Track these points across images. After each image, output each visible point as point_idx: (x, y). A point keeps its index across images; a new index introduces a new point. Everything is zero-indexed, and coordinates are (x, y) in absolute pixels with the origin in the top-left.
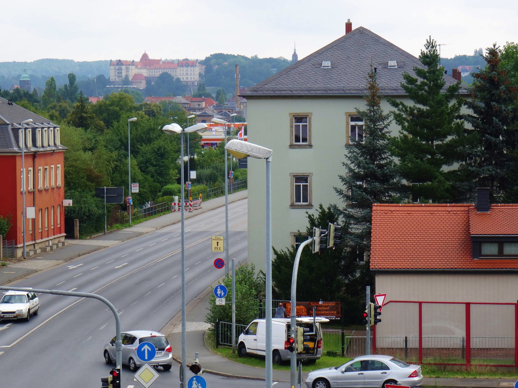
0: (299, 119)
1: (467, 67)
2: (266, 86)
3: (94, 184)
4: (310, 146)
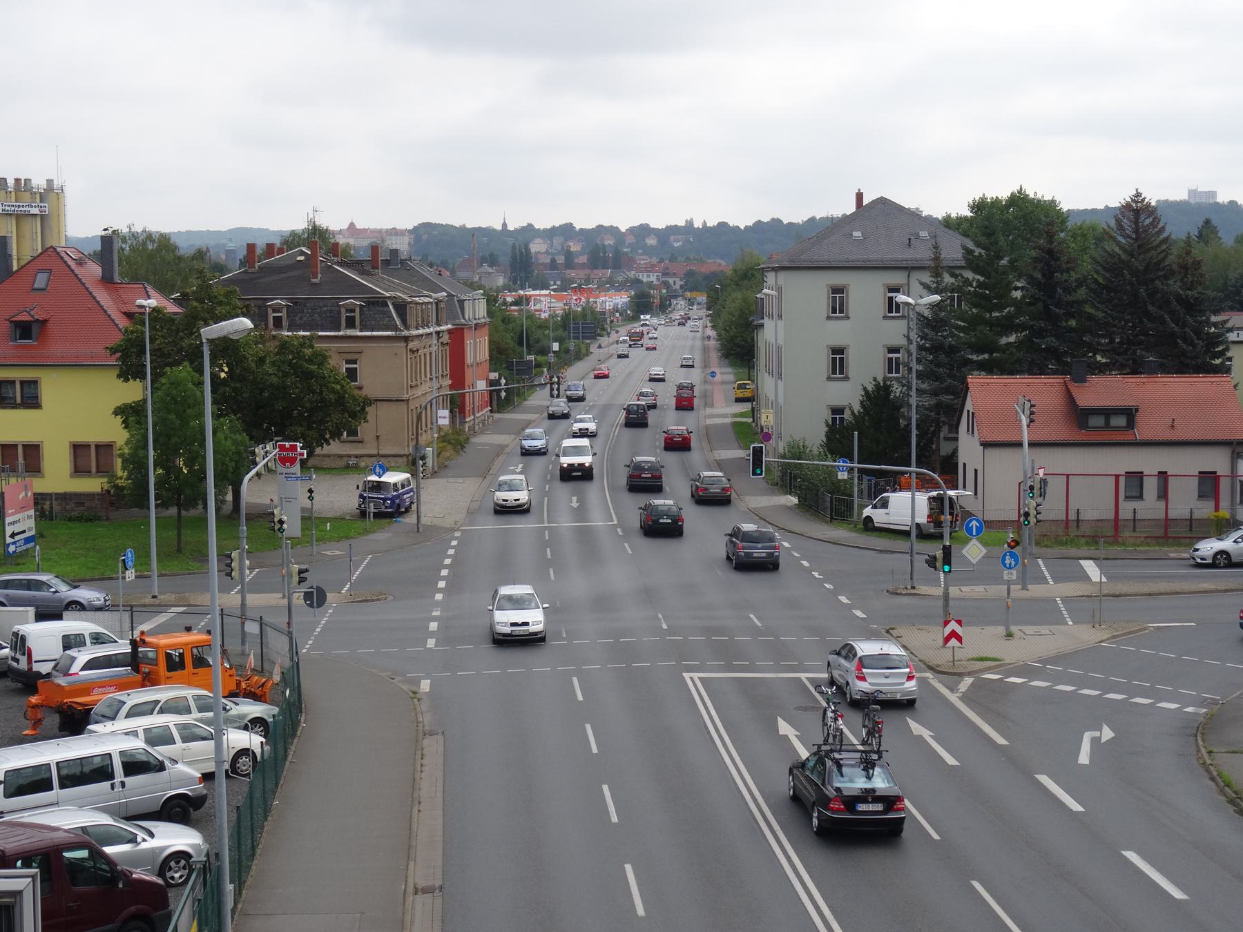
0: (837, 290)
1: (680, 237)
2: (801, 257)
3: (503, 357)
4: (848, 318)
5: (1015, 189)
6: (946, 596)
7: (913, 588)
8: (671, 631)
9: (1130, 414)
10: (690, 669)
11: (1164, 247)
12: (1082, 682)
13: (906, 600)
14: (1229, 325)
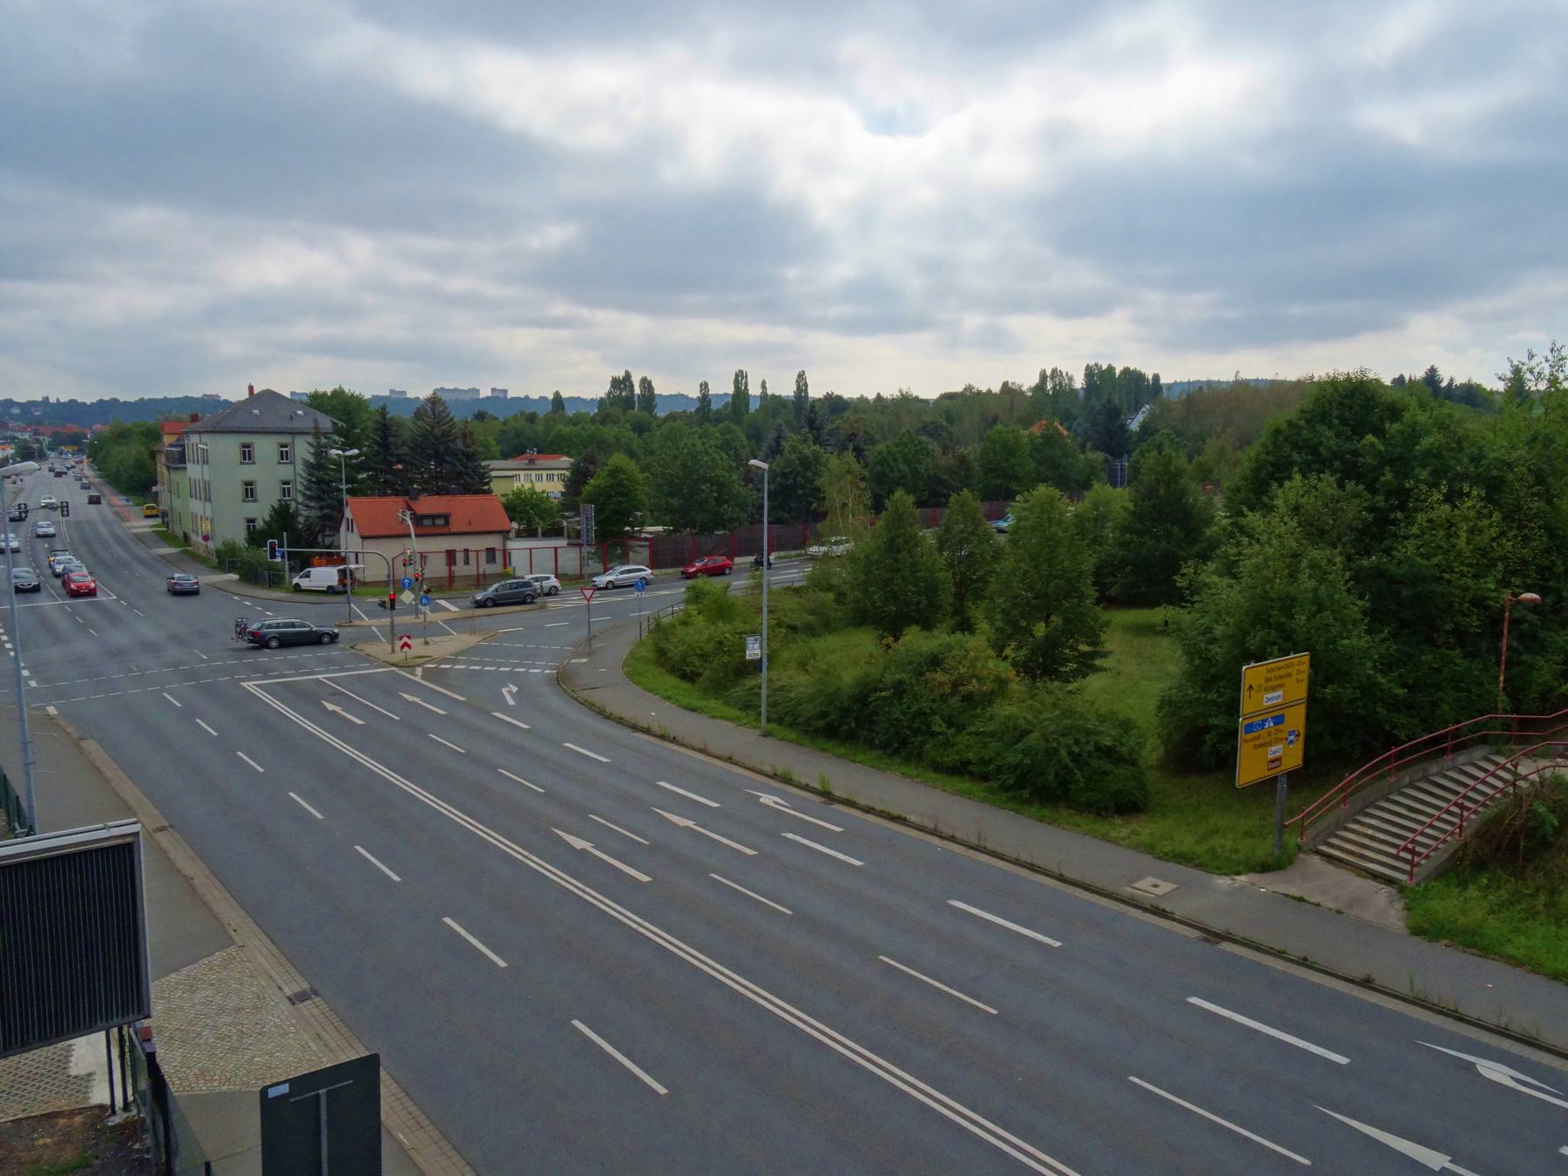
0: (245, 446)
4: (254, 463)
5: (337, 387)
6: (392, 623)
7: (351, 622)
8: (210, 660)
9: (446, 517)
10: (244, 680)
11: (450, 424)
12: (484, 664)
13: (349, 629)
14: (490, 467)
